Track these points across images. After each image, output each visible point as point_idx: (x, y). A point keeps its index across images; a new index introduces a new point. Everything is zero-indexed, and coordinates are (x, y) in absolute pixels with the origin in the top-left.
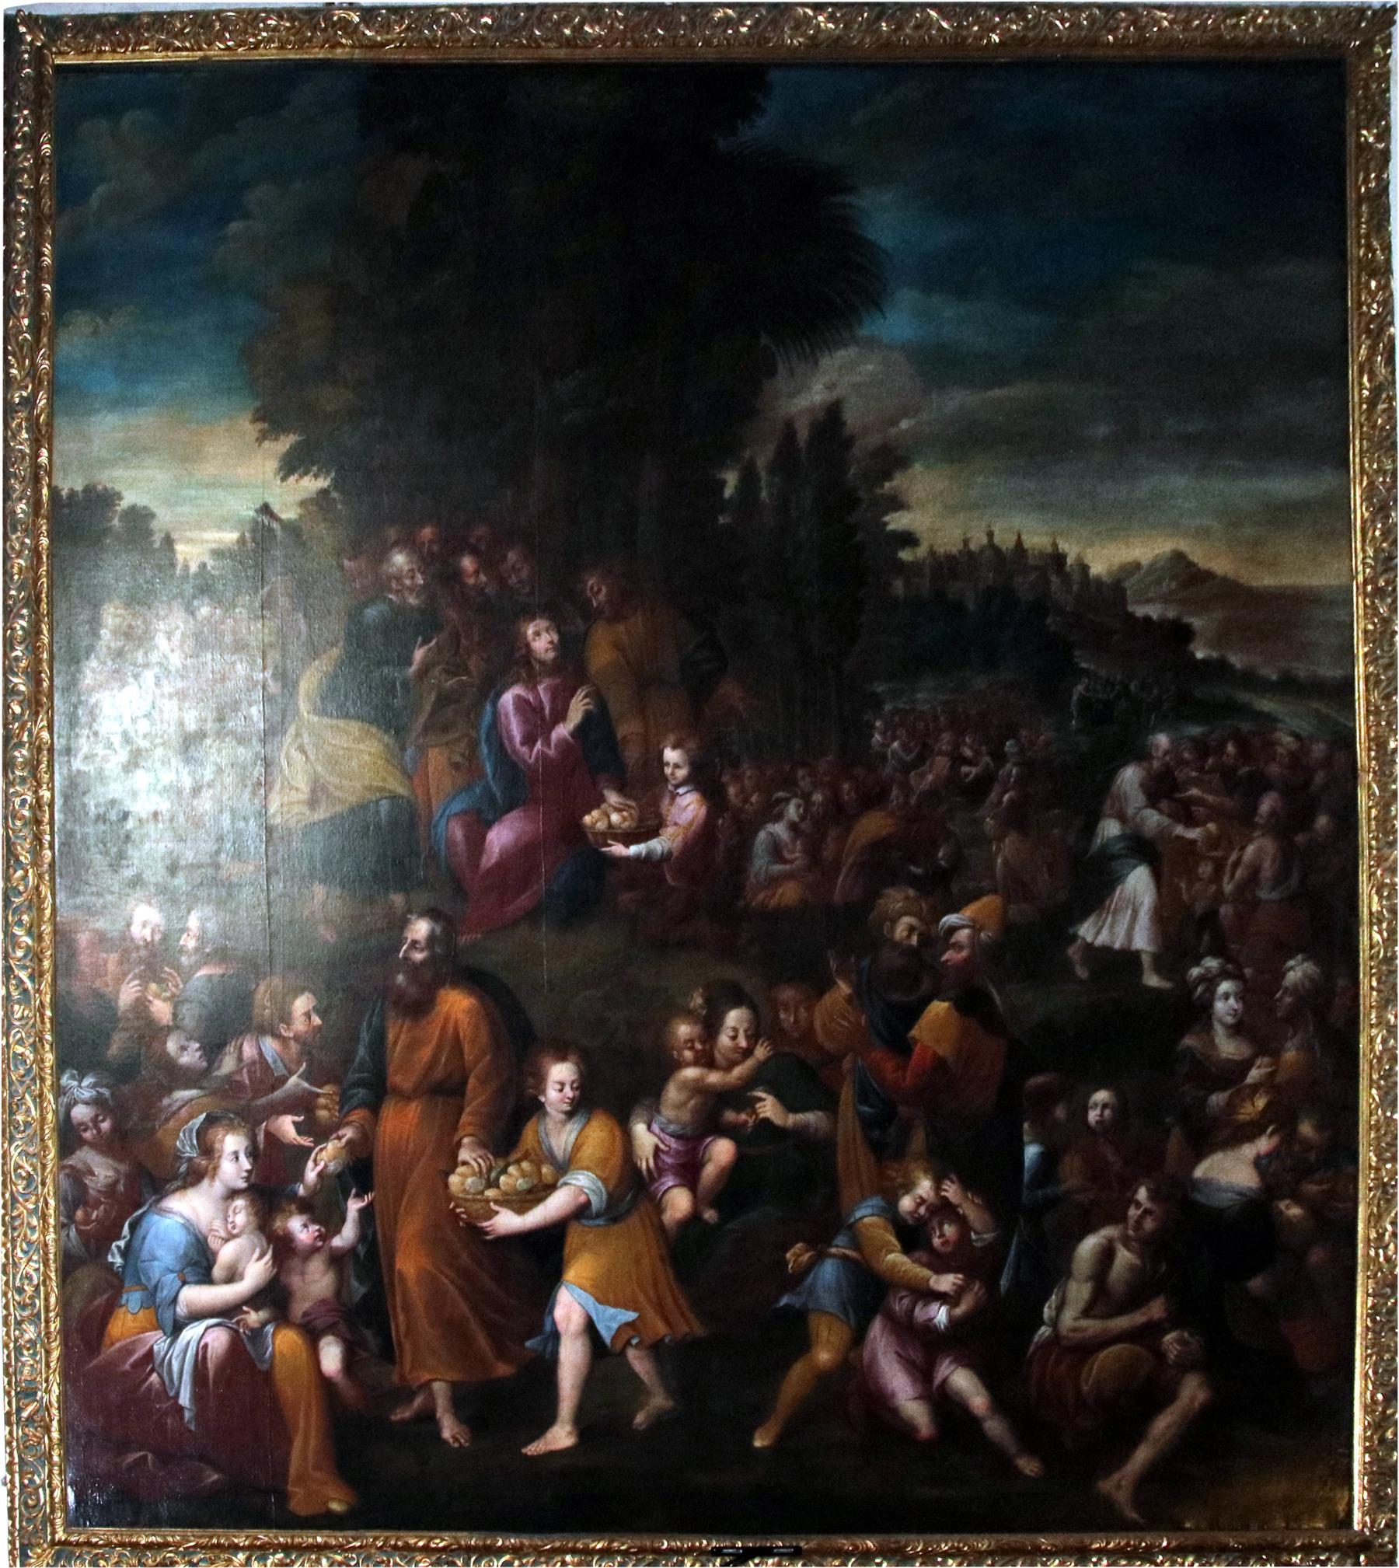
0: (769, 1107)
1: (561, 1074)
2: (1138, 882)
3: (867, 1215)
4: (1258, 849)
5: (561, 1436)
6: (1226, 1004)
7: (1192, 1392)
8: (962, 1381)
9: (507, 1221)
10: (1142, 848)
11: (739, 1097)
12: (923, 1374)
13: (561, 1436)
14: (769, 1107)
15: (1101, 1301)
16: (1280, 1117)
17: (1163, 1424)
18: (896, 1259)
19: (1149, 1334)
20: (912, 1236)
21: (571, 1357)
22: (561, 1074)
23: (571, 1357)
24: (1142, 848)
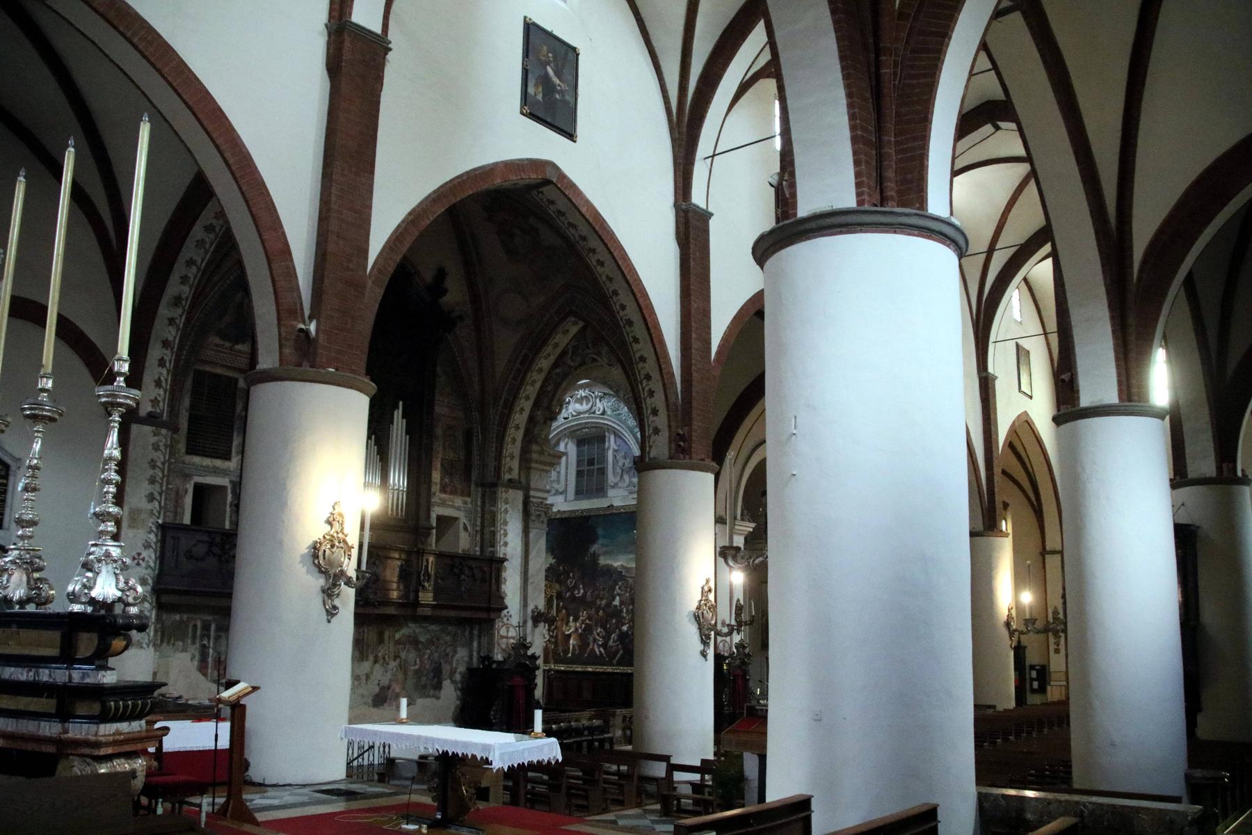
0: (587, 621)
1: (571, 618)
2: (618, 598)
3: (595, 632)
4: (628, 594)
5: (570, 655)
6: (625, 611)
7: (621, 652)
8: (602, 650)
9: (567, 633)
10: (618, 594)
11: (585, 620)
12: (599, 648)
13: (570, 655)
14: (587, 621)
15: (614, 642)
16: (629, 623)
17: (619, 655)
18: (597, 637)
19: (617, 645)
20: (598, 634)
21: (571, 646)
22: (571, 618)
23: (571, 646)
24: (618, 594)
